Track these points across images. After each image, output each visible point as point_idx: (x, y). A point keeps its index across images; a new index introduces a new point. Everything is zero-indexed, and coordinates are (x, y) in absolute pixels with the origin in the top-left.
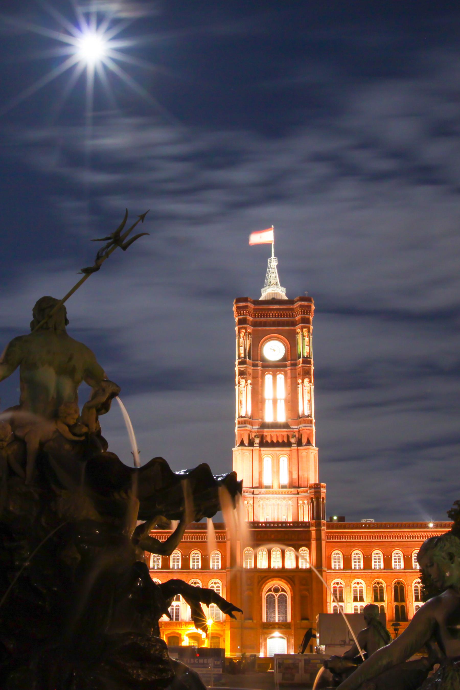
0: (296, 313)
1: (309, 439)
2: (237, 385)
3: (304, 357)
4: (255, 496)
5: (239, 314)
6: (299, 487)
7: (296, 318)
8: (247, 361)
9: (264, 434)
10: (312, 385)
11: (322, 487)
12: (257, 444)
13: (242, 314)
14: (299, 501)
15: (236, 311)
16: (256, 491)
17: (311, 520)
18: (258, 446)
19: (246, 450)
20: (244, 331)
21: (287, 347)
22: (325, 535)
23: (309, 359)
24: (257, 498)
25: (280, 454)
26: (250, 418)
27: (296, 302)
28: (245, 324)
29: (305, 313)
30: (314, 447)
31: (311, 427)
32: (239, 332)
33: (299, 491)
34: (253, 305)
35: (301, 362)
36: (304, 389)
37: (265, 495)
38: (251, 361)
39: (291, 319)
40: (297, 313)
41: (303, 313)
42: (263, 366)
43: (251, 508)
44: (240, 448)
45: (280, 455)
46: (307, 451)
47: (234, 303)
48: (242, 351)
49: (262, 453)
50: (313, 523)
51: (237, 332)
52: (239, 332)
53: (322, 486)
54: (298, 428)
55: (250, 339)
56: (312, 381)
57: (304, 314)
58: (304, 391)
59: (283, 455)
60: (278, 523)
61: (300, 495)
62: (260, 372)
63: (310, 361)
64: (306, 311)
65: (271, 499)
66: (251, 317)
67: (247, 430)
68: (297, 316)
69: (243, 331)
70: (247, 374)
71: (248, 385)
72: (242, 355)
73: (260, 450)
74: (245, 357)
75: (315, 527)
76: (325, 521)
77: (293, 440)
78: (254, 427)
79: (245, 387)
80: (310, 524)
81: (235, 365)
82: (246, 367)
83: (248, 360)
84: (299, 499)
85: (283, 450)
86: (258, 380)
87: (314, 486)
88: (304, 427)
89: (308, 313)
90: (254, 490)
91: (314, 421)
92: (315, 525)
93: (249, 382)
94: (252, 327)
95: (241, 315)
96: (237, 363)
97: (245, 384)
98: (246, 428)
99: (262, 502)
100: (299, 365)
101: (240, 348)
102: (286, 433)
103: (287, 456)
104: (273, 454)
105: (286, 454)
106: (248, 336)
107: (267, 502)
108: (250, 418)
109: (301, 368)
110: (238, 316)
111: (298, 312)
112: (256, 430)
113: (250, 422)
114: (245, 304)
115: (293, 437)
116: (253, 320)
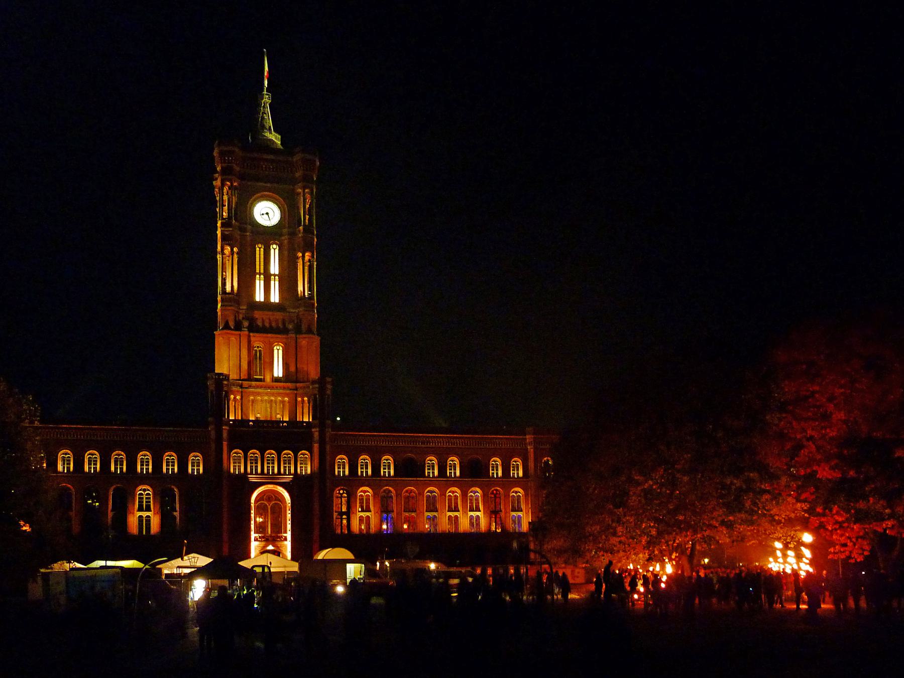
4: (243, 389)
5: (223, 161)
6: (296, 381)
16: (246, 383)
19: (232, 334)
21: (284, 210)
24: (245, 392)
35: (302, 231)
52: (223, 185)
61: (300, 391)
73: (249, 336)
74: (229, 217)
79: (229, 257)
82: (232, 230)
93: (235, 249)
95: (225, 163)
101: (224, 207)
114: (230, 148)
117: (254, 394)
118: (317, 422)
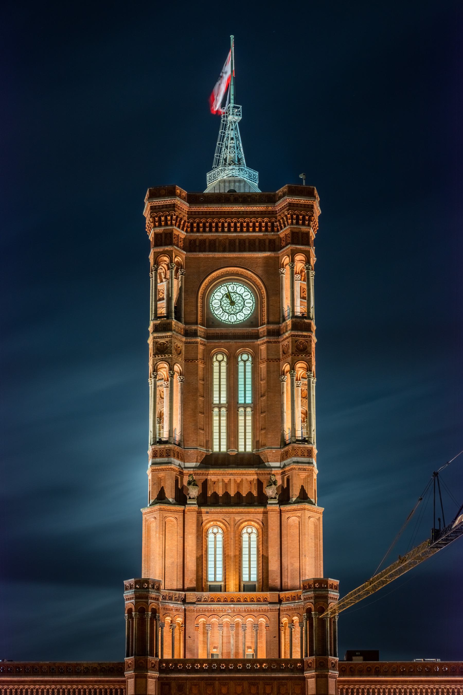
0: (279, 221)
1: (304, 489)
2: (152, 375)
3: (294, 316)
6: (281, 590)
7: (279, 233)
8: (173, 323)
9: (209, 477)
10: (312, 375)
11: (331, 588)
12: (193, 498)
13: (163, 223)
14: (280, 617)
15: (151, 217)
16: (191, 596)
17: (306, 656)
18: (196, 502)
20: (166, 259)
22: (337, 689)
23: (306, 321)
25: (241, 521)
26: (179, 445)
27: (280, 198)
28: (171, 244)
29: (301, 222)
30: (315, 505)
31: (310, 463)
32: (157, 263)
33: (281, 597)
34: (188, 205)
35: (290, 327)
36: (295, 385)
37: (209, 606)
38: (181, 325)
39: (270, 235)
40: (281, 221)
41: (294, 221)
42: (208, 337)
43: (180, 633)
44: (157, 507)
45: (242, 523)
46: (299, 515)
47: (145, 201)
48: (162, 304)
49: (204, 519)
50: (310, 661)
51: (152, 261)
53: (330, 585)
54: (282, 466)
55: (180, 276)
56: (314, 368)
57: (297, 223)
58: (295, 388)
59: (249, 522)
60: (236, 661)
62: (201, 348)
63: (310, 324)
64: (301, 217)
65: (222, 614)
66: (183, 229)
67: (172, 469)
68: (281, 229)
69: (165, 261)
70: (174, 351)
71: (175, 376)
72: (163, 311)
73: (199, 513)
74: (168, 316)
75: (314, 671)
76: (337, 659)
77: (270, 492)
78: (187, 465)
80: (305, 662)
81: (148, 332)
82: (171, 336)
83: (174, 322)
84: (281, 613)
85: (249, 513)
86: (197, 365)
87: (314, 586)
88: (294, 462)
89: (307, 222)
90: (185, 595)
91: (315, 451)
92: (314, 665)
93: (177, 368)
94: (185, 253)
95: (160, 225)
96: (151, 329)
97: (168, 372)
98: (170, 464)
99: (202, 620)
100: (284, 333)
102: (256, 477)
103: (258, 523)
104: (227, 519)
105: (255, 520)
106: (177, 271)
107: (214, 620)
108: (179, 445)
109: (290, 340)
110: (155, 226)
111: (285, 218)
112: (192, 469)
113: (178, 453)
114: (168, 201)
115: (271, 485)
116: (186, 236)
117: (203, 613)
118: (311, 659)
